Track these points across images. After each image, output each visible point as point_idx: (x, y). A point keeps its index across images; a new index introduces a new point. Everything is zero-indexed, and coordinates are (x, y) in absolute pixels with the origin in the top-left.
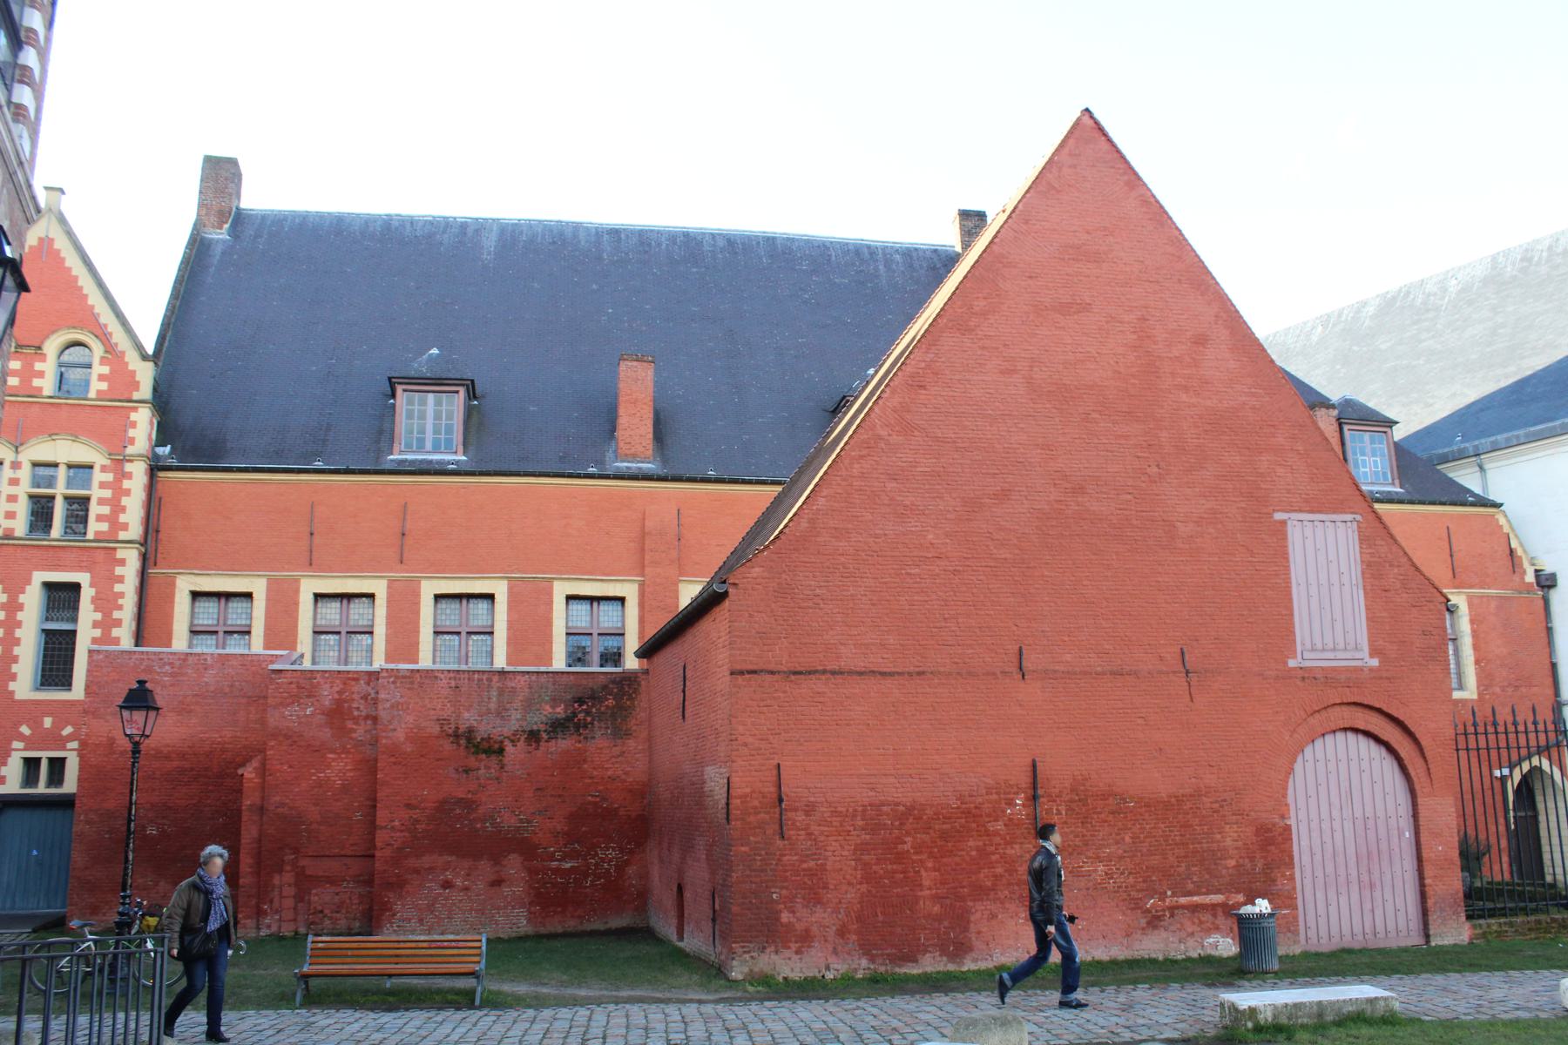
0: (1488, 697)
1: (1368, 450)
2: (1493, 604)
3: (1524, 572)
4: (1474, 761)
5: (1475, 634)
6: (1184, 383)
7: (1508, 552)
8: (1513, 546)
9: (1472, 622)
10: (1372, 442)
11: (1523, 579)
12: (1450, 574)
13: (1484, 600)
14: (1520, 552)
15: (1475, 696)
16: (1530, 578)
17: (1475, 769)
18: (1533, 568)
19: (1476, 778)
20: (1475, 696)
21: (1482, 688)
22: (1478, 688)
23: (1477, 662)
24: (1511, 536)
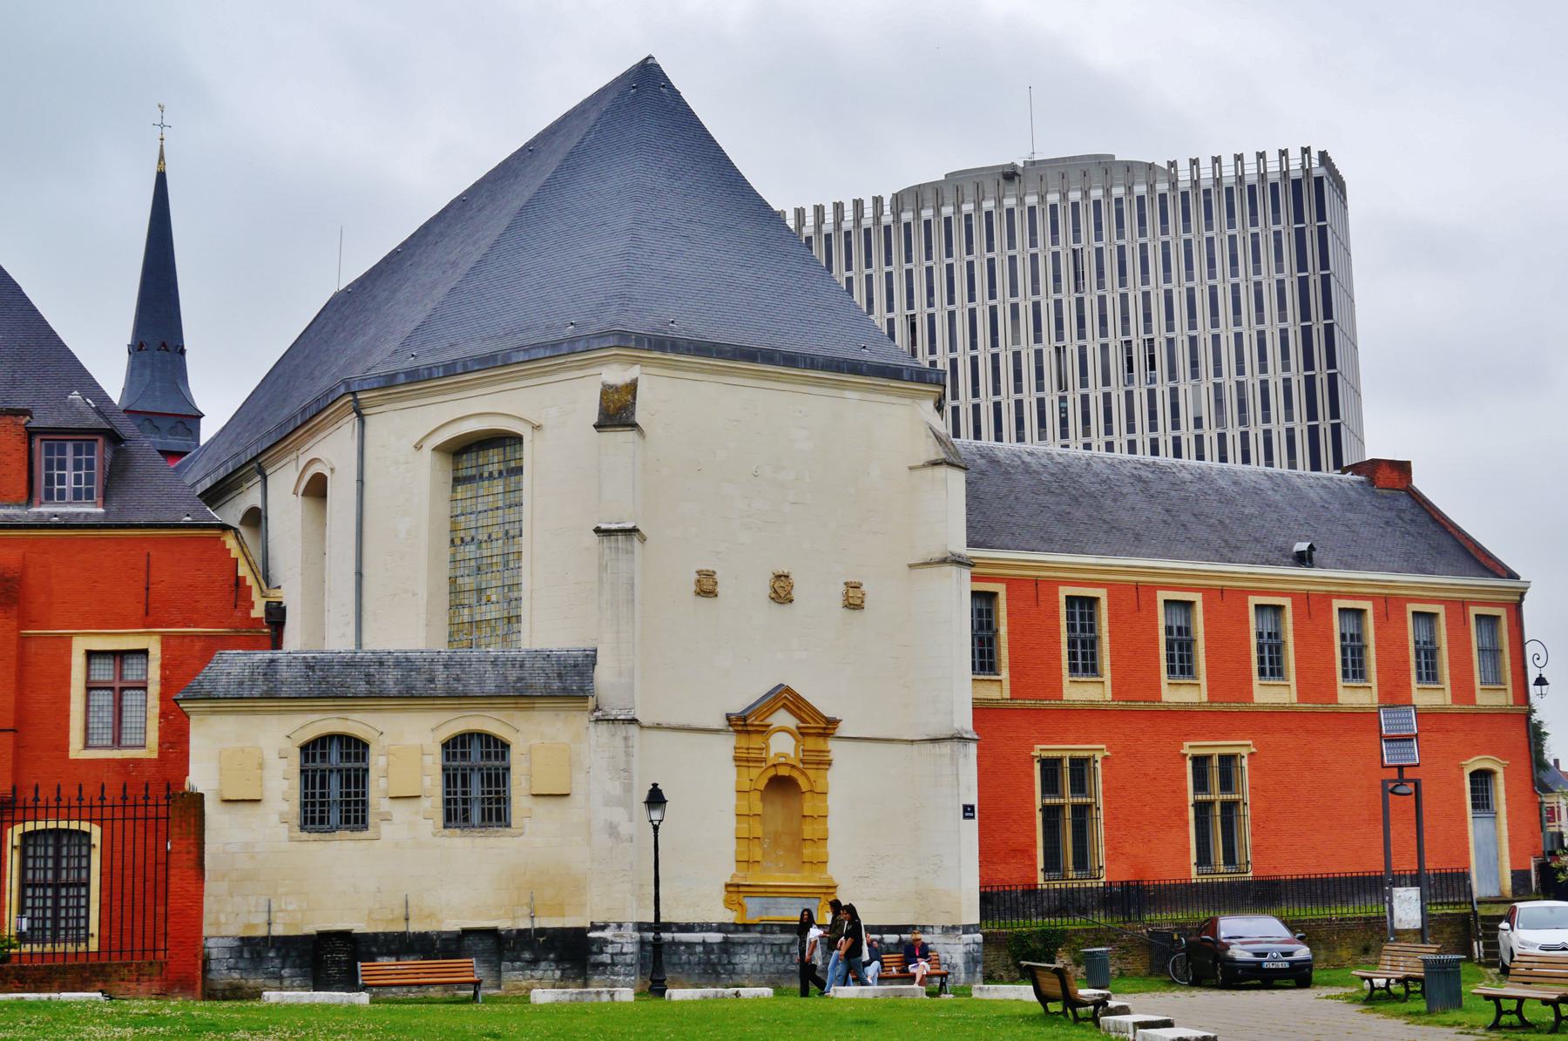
0: (173, 755)
1: (70, 464)
2: (198, 645)
3: (252, 605)
4: (140, 830)
5: (165, 681)
6: (446, 290)
7: (233, 581)
8: (240, 573)
9: (163, 667)
10: (77, 451)
11: (249, 613)
12: (142, 612)
13: (187, 640)
14: (250, 581)
15: (155, 755)
16: (258, 612)
17: (139, 841)
18: (264, 601)
19: (140, 851)
20: (155, 755)
21: (167, 745)
22: (160, 745)
23: (163, 715)
24: (242, 562)
